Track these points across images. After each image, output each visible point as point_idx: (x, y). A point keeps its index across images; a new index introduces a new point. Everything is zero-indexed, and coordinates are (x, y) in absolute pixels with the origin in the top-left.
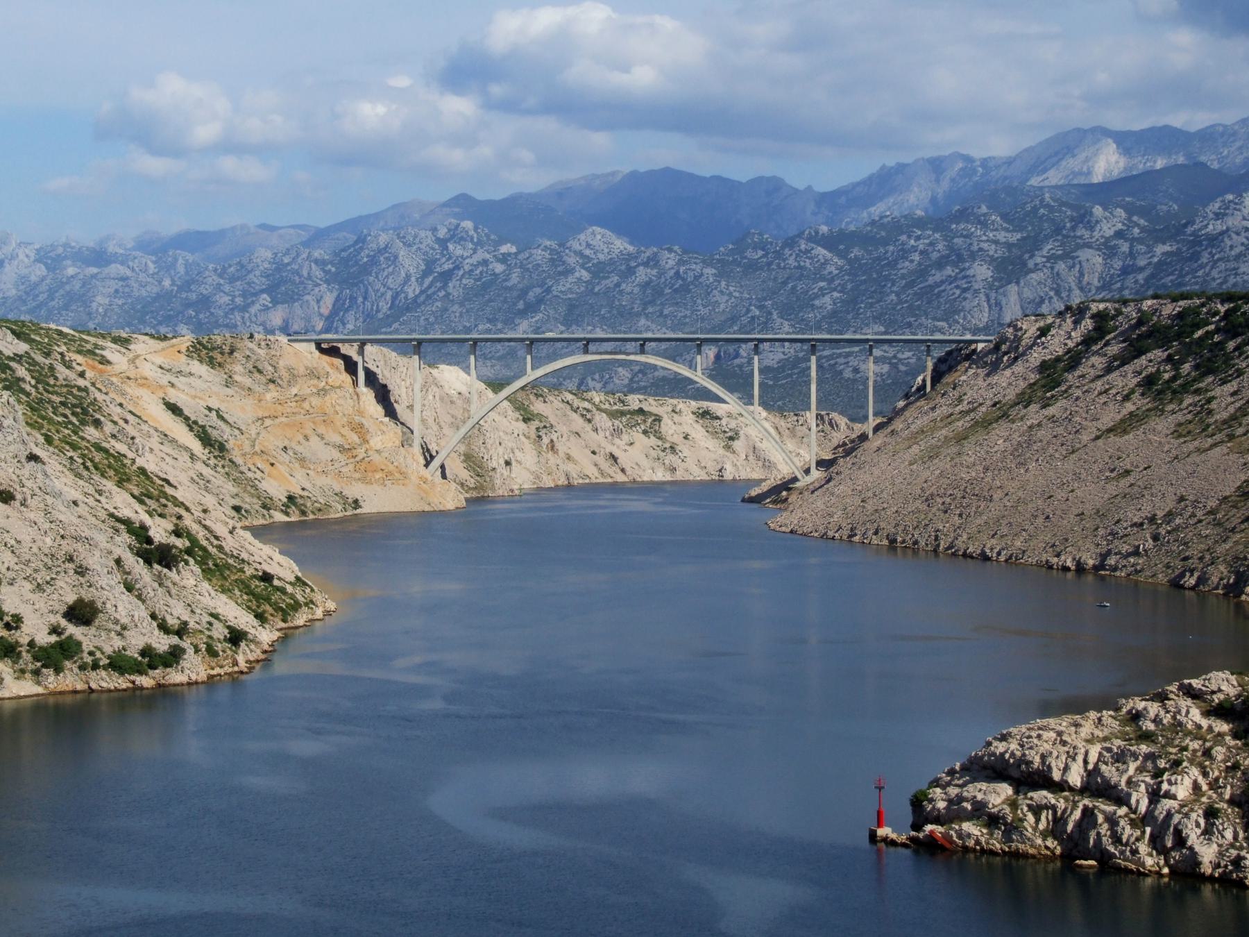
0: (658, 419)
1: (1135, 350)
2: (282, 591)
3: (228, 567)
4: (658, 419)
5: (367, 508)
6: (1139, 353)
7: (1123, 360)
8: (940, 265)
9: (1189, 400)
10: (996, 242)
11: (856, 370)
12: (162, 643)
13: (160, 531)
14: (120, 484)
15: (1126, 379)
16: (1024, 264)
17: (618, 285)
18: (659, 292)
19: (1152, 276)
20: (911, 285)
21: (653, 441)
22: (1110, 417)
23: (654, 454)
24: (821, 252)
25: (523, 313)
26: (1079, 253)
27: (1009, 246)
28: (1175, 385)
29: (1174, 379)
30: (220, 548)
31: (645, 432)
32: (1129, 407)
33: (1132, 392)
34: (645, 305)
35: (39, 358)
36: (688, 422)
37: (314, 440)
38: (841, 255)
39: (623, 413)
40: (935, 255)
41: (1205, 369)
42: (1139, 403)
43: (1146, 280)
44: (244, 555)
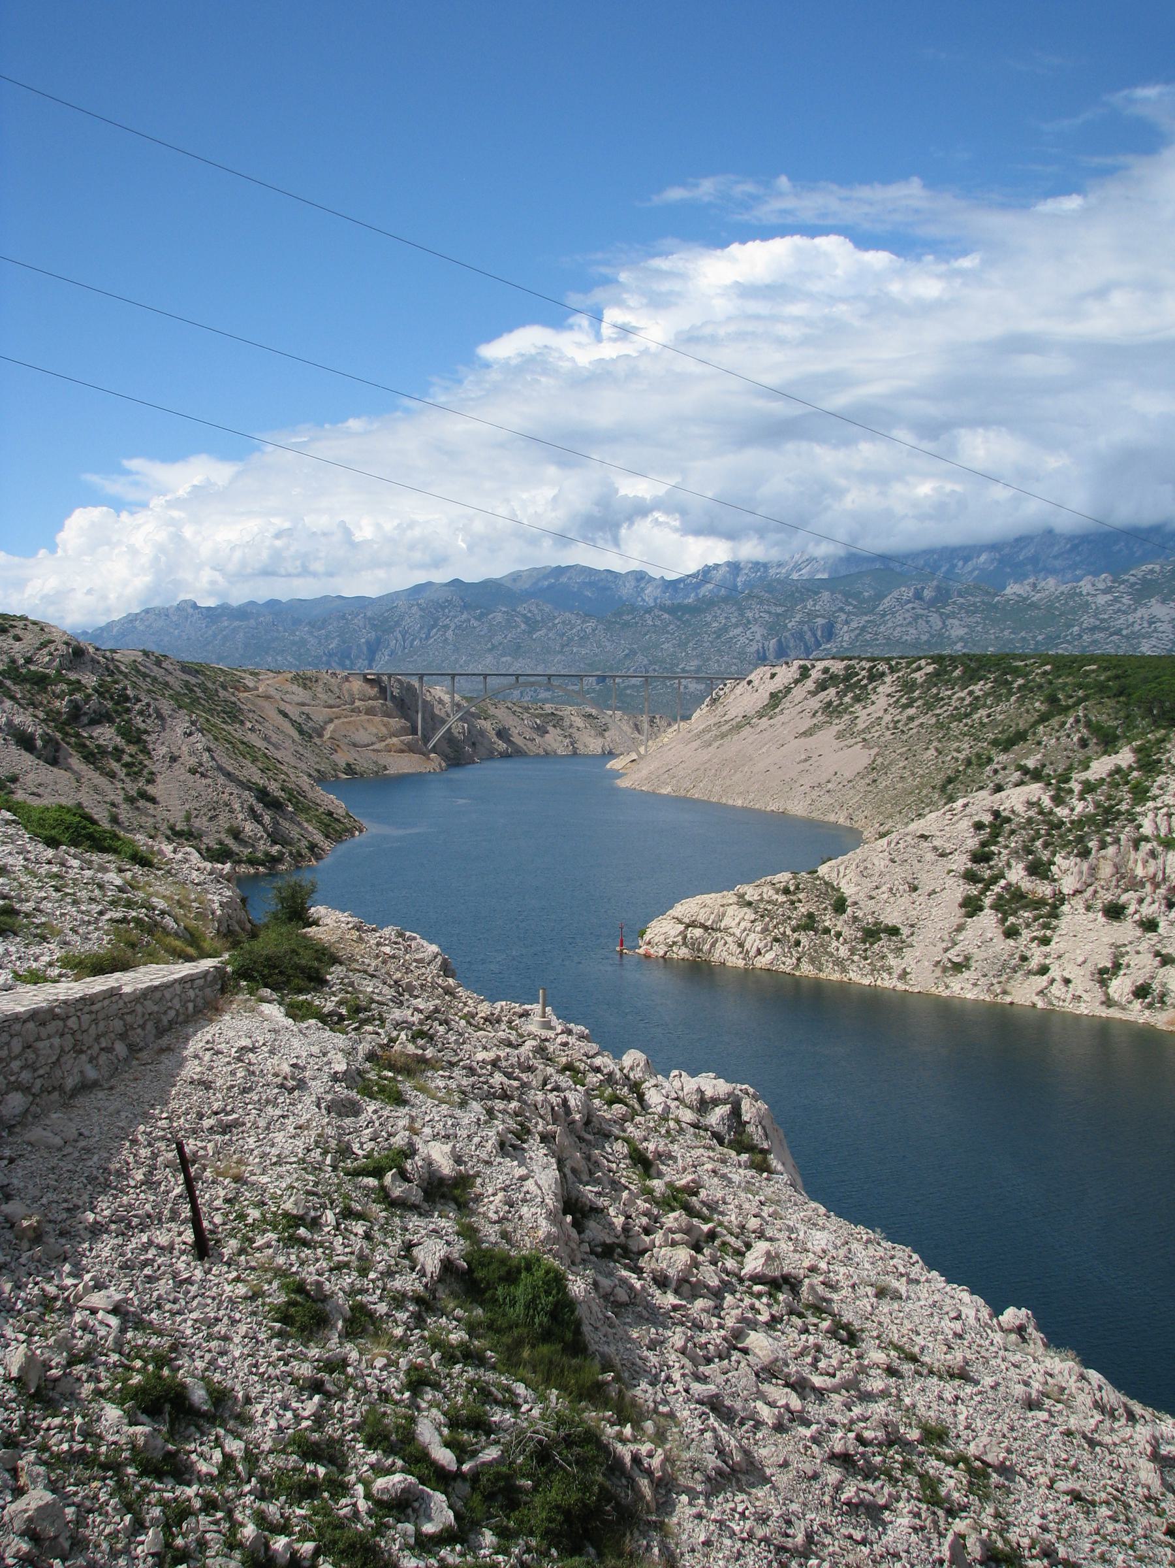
0: (562, 719)
1: (822, 686)
2: (338, 820)
3: (309, 808)
4: (562, 719)
5: (391, 771)
6: (824, 689)
7: (814, 693)
8: (736, 626)
9: (846, 717)
10: (769, 613)
11: (686, 687)
12: (275, 850)
13: (273, 788)
14: (253, 762)
15: (815, 703)
16: (786, 625)
17: (547, 635)
18: (570, 640)
19: (859, 634)
20: (718, 637)
21: (559, 731)
22: (808, 723)
23: (560, 738)
24: (666, 616)
25: (490, 650)
26: (818, 620)
27: (778, 615)
28: (840, 709)
29: (838, 706)
30: (305, 797)
31: (554, 726)
32: (815, 721)
33: (817, 712)
34: (563, 646)
35: (210, 685)
36: (579, 722)
37: (362, 731)
38: (679, 619)
39: (542, 715)
40: (734, 620)
41: (857, 699)
42: (820, 718)
43: (856, 636)
44: (318, 801)
